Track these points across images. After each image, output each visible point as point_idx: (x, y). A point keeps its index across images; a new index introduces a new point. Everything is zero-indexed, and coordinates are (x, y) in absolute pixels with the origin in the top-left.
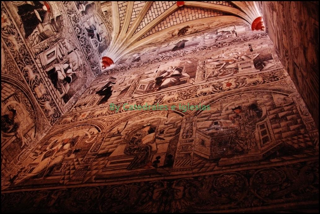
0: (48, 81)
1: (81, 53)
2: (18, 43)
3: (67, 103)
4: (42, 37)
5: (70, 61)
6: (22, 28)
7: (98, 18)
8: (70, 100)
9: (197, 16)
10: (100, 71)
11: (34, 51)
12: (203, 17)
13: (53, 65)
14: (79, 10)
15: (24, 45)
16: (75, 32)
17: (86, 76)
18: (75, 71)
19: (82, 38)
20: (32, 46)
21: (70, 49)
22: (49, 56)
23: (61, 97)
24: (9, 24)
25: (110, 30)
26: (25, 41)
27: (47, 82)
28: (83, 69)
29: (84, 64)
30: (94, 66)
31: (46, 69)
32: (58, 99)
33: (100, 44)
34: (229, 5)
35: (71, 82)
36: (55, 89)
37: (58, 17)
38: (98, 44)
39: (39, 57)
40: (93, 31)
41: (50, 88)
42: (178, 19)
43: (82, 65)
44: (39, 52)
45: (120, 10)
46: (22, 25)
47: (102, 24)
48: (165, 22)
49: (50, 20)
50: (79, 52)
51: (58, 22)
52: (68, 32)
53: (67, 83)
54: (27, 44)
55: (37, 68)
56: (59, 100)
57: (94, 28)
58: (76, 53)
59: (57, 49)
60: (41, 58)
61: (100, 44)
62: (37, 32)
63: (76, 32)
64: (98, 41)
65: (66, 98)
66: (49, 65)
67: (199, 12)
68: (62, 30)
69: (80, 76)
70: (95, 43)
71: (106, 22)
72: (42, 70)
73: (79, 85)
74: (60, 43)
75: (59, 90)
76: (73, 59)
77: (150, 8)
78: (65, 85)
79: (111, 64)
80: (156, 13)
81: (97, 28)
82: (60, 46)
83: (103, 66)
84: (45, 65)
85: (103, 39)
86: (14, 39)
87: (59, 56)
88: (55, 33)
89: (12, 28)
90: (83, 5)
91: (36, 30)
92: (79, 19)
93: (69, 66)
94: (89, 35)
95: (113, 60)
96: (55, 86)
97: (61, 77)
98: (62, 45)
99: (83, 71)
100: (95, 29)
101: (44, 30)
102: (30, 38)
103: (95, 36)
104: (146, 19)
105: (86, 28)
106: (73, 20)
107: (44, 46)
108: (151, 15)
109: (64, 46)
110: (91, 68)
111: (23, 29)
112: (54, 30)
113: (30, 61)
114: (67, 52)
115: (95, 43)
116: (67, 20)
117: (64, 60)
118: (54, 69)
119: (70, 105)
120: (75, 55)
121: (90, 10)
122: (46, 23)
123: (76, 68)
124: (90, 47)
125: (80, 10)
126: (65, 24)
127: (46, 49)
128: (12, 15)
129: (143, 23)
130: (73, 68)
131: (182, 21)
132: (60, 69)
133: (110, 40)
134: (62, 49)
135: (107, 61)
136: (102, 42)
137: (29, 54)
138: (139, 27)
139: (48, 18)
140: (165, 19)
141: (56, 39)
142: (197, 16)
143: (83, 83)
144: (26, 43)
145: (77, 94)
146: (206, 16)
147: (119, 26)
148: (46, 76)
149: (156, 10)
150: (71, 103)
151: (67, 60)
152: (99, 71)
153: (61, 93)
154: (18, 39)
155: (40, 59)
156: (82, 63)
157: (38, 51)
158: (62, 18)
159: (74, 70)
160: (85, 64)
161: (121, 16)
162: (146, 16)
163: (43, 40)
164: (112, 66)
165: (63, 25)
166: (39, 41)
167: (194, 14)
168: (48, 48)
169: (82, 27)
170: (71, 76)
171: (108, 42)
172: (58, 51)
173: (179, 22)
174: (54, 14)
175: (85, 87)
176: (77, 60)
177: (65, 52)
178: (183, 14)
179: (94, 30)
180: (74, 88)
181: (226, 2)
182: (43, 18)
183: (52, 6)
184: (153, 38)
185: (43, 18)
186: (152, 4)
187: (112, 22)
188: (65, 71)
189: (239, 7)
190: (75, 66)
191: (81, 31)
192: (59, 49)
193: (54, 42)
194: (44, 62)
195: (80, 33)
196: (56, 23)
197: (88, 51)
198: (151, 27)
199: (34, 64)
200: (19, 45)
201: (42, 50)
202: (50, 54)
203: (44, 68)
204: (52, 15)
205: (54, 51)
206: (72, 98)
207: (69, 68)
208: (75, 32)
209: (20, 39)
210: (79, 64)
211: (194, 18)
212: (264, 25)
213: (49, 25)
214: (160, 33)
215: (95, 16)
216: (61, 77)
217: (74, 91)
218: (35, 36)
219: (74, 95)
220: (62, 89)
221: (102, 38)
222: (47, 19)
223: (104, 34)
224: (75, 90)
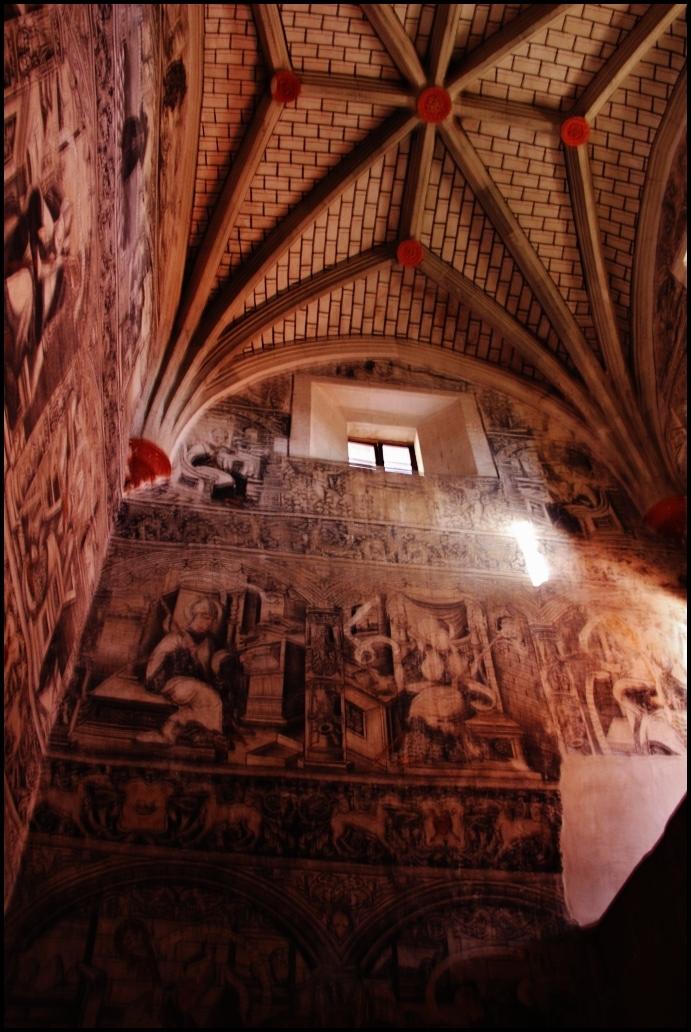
67: (225, 146)
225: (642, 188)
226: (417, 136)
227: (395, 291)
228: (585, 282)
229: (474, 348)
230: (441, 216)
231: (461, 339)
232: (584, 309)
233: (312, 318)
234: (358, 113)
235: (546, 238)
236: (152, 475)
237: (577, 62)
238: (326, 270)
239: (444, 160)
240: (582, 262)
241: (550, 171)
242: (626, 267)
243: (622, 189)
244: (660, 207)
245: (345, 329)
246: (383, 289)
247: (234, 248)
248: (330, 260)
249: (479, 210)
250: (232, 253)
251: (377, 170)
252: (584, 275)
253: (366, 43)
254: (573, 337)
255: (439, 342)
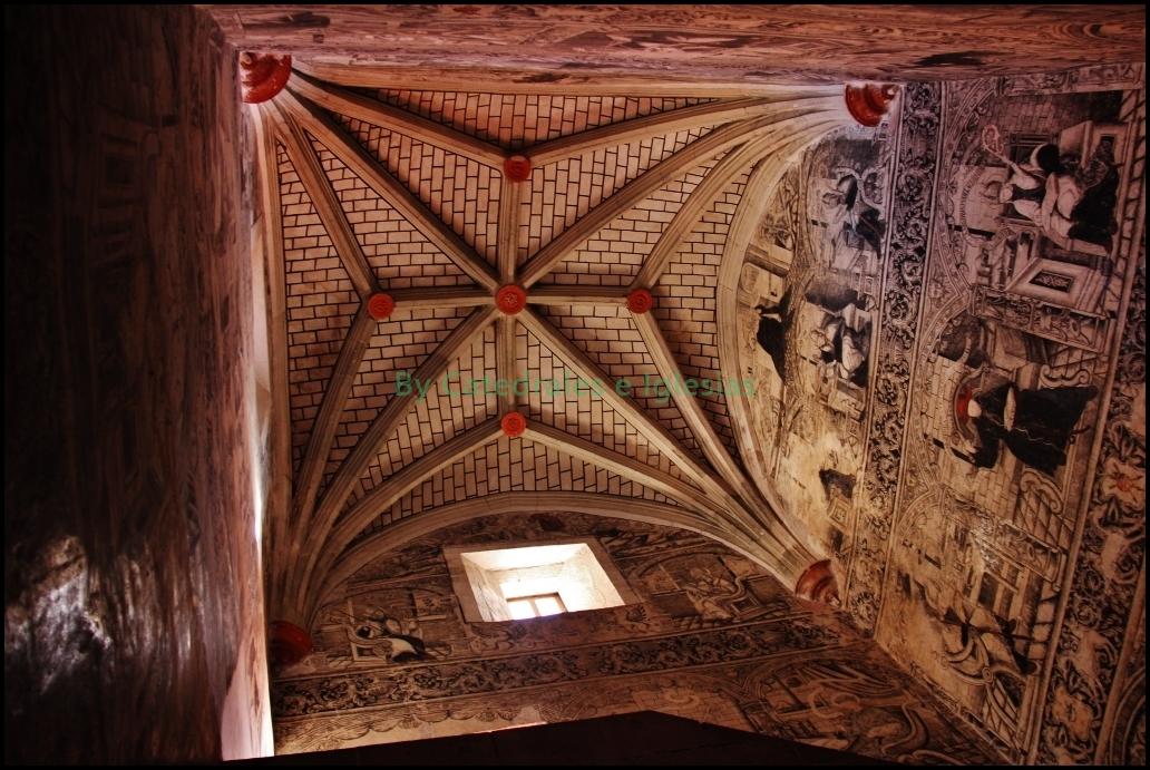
0: (1125, 218)
1: (942, 199)
2: (1131, 399)
3: (1116, 87)
4: (1044, 351)
5: (997, 210)
6: (1086, 422)
7: (819, 251)
8: (1097, 88)
9: (472, 104)
10: (908, 89)
11: (1099, 337)
12: (452, 96)
13: (1068, 249)
14: (867, 320)
15: (1117, 379)
16: (922, 274)
17: (977, 116)
18: (1004, 166)
19: (911, 240)
20: (1093, 356)
21: (973, 242)
22: (1064, 284)
23: (1123, 128)
24: (1112, 460)
25: (797, 182)
26: (1104, 386)
27: (1134, 219)
28: (972, 147)
29: (956, 160)
30: (922, 123)
31: (1104, 259)
32: (1138, 131)
33: (860, 172)
34: (350, 122)
35: (1045, 144)
36: (1124, 173)
37: (954, 357)
38: (864, 178)
39: (1099, 311)
40: (858, 226)
41: (1137, 191)
42: (544, 112)
43: (967, 164)
44: (1087, 322)
45: (730, 218)
46: (1079, 426)
47: (815, 223)
48: (593, 120)
49: (979, 370)
50: (950, 207)
51: (961, 345)
52: (947, 296)
53: (1061, 152)
54: (1108, 373)
55: (1133, 288)
56: (1135, 125)
57: (851, 236)
58: (963, 214)
59: (1020, 279)
60: (1093, 302)
61: (860, 172)
62: (1047, 377)
63: (920, 270)
64: (860, 186)
65: (1103, 108)
66: (1086, 262)
67: (459, 116)
68: (964, 315)
69: (997, 136)
70: (874, 187)
71: (797, 214)
72: (1120, 268)
73: (1023, 112)
74: (996, 287)
75: (1112, 157)
76: (985, 206)
77: (626, 185)
78: (1074, 154)
79: (857, 91)
80: (611, 158)
81: (841, 224)
82: (1002, 280)
83: (892, 97)
84: (1098, 272)
85: (839, 177)
86: (1134, 417)
87: (1029, 256)
88: (992, 326)
89: (1114, 447)
90: (848, 323)
91: (1043, 383)
92: (884, 297)
93: (1014, 198)
94: (881, 227)
95: (842, 98)
96: (1112, 182)
97: (1070, 191)
98: (996, 278)
99: (976, 142)
100: (847, 226)
101: (1022, 363)
102: (1083, 381)
103: (863, 209)
104: (657, 154)
105: (879, 257)
106: (906, 307)
107: (1055, 323)
108: (633, 163)
109: (988, 269)
110: (938, 124)
111: (1085, 418)
112: (990, 336)
113: (1136, 325)
114: (992, 243)
115: (874, 187)
116: (927, 325)
117: (1018, 230)
118: (1073, 234)
119: (1111, 72)
120: (969, 208)
121: (834, 292)
122: (1002, 373)
123: (994, 170)
124: (900, 191)
125: (865, 315)
126: (942, 322)
127: (1056, 311)
128: (1086, 473)
129: (669, 146)
130: (1003, 181)
131: (532, 100)
132: (1055, 218)
133: (815, 153)
134: (999, 266)
135: (865, 105)
136: (848, 171)
137: (1122, 345)
138: (691, 139)
139: (982, 380)
140: (589, 127)
141: (1002, 310)
142: (472, 104)
143: (1005, 103)
144: (1106, 380)
145: (1053, 86)
146: (438, 98)
147: (759, 173)
148: (1121, 237)
149: (610, 171)
150: (1099, 73)
151: (1007, 220)
152: (914, 92)
153: (1109, 140)
154: (1122, 407)
155: (1100, 302)
156: (963, 169)
157: (1086, 325)
158: (939, 344)
159: (1006, 171)
160: (954, 156)
161: (736, 199)
162: (653, 163)
163: (1046, 341)
164: (859, 84)
165: (951, 326)
166: (1060, 349)
167: (483, 112)
168: (1045, 307)
169: (890, 270)
170: (1028, 162)
171: (825, 154)
172: (1018, 272)
173: (544, 102)
174: (957, 376)
175: (1002, 84)
176: (972, 190)
177: (998, 253)
178: (518, 122)
179: (854, 227)
180: (1051, 115)
181: (359, 131)
182: (1001, 393)
183: (948, 396)
184: (659, 88)
185: (1001, 393)
186: (614, 194)
187: (776, 199)
188: (1038, 195)
189: (315, 120)
190: (992, 179)
191: (903, 262)
192: (1011, 273)
193: (1012, 307)
194: (1093, 284)
195: (909, 259)
196: (968, 347)
197: (916, 186)
198: (650, 128)
199: (1133, 305)
200: (1134, 391)
201: (1072, 321)
202: (1051, 287)
203: (1109, 270)
204: (964, 376)
205: (1033, 282)
206: (1080, 89)
207: (1018, 193)
208: (922, 274)
209: (1117, 405)
210: (972, 173)
211: (485, 99)
212: (243, 74)
213: (993, 361)
214: (625, 92)
215: (824, 262)
216: (1070, 191)
217: (1057, 105)
218: (1062, 371)
219: (1064, 92)
220: (1093, 150)
221: (840, 183)
222: (989, 381)
223: (824, 186)
224: (1047, 106)
225: (477, 496)
226: (477, 288)
227: (331, 299)
228: (389, 477)
229: (297, 393)
230: (409, 327)
231: (303, 376)
232: (368, 485)
233: (303, 220)
234: (486, 233)
235: (414, 429)
236: (254, 82)
237: (559, 408)
238: (351, 226)
239: (456, 317)
240: (404, 468)
241: (469, 414)
242: (412, 510)
243: (471, 479)
244: (469, 518)
245: (290, 256)
246: (332, 286)
247: (374, 134)
248: (358, 229)
249: (421, 360)
250: (369, 133)
251: (441, 259)
252: (394, 474)
253: (546, 232)
254: (348, 487)
255: (292, 355)
